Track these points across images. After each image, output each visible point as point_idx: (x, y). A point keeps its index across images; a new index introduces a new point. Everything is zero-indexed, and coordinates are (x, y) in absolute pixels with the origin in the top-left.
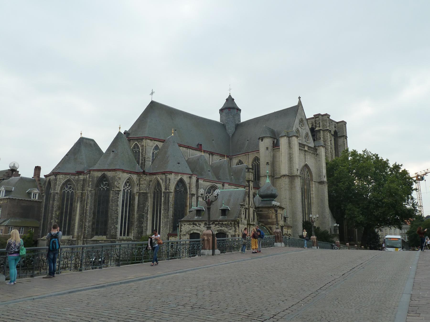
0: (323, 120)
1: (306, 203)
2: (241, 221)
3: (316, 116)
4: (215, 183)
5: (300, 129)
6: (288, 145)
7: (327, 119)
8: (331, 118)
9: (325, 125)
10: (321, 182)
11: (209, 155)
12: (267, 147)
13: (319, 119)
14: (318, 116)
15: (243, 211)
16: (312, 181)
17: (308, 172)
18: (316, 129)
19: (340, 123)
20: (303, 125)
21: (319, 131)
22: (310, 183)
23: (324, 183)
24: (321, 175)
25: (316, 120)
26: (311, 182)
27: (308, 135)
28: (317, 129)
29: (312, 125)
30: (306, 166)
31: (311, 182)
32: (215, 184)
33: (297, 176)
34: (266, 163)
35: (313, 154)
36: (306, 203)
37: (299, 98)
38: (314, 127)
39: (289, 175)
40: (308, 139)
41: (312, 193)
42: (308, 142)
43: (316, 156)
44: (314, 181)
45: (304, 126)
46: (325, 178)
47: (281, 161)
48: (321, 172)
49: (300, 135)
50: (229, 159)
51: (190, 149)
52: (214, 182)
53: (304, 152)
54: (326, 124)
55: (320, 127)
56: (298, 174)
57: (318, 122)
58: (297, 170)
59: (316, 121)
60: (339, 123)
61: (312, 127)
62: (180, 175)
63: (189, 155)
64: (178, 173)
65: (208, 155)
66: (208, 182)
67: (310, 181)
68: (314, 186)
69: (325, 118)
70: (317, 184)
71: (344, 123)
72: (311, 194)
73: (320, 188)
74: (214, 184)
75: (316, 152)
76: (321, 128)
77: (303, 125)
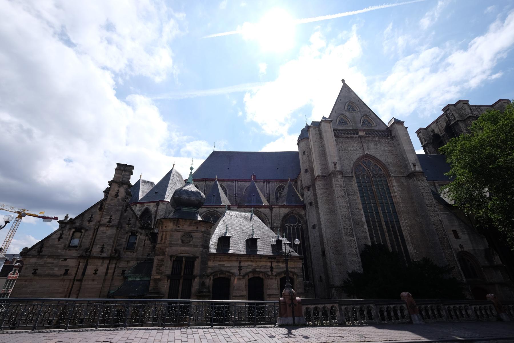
0: (458, 110)
1: (381, 214)
2: (40, 251)
3: (446, 109)
4: (215, 208)
5: (347, 114)
6: (318, 137)
7: (463, 106)
8: (470, 103)
9: (463, 114)
10: (410, 174)
11: (264, 183)
12: (303, 151)
13: (451, 110)
14: (447, 108)
15: (61, 234)
16: (390, 176)
17: (378, 166)
18: (450, 123)
19: (497, 105)
20: (355, 109)
21: (457, 123)
22: (387, 180)
23: (414, 175)
24: (407, 164)
25: (447, 113)
26: (388, 179)
27: (369, 118)
28: (452, 123)
29: (447, 122)
30: (367, 156)
31: (388, 179)
32: (216, 209)
33: (334, 173)
34: (305, 171)
35: (382, 138)
36: (381, 214)
37: (343, 81)
38: (449, 123)
39: (324, 174)
40: (371, 122)
41: (394, 196)
42: (372, 126)
43: (393, 140)
44: (394, 177)
45: (358, 108)
46: (417, 167)
47: (313, 160)
48: (406, 159)
49: (349, 120)
50: (293, 183)
51: (236, 182)
52: (212, 208)
53: (360, 139)
54: (463, 112)
55: (455, 119)
56: (337, 169)
57: (451, 115)
58: (335, 165)
59: (447, 114)
60: (495, 105)
61: (447, 124)
62: (145, 204)
63: (235, 187)
64: (144, 203)
65: (262, 184)
66: (203, 208)
67: (387, 178)
68: (394, 183)
69: (460, 105)
70: (404, 181)
71: (502, 102)
72: (393, 198)
73: (412, 185)
74: (214, 209)
75: (391, 135)
76: (457, 119)
77: (356, 107)
